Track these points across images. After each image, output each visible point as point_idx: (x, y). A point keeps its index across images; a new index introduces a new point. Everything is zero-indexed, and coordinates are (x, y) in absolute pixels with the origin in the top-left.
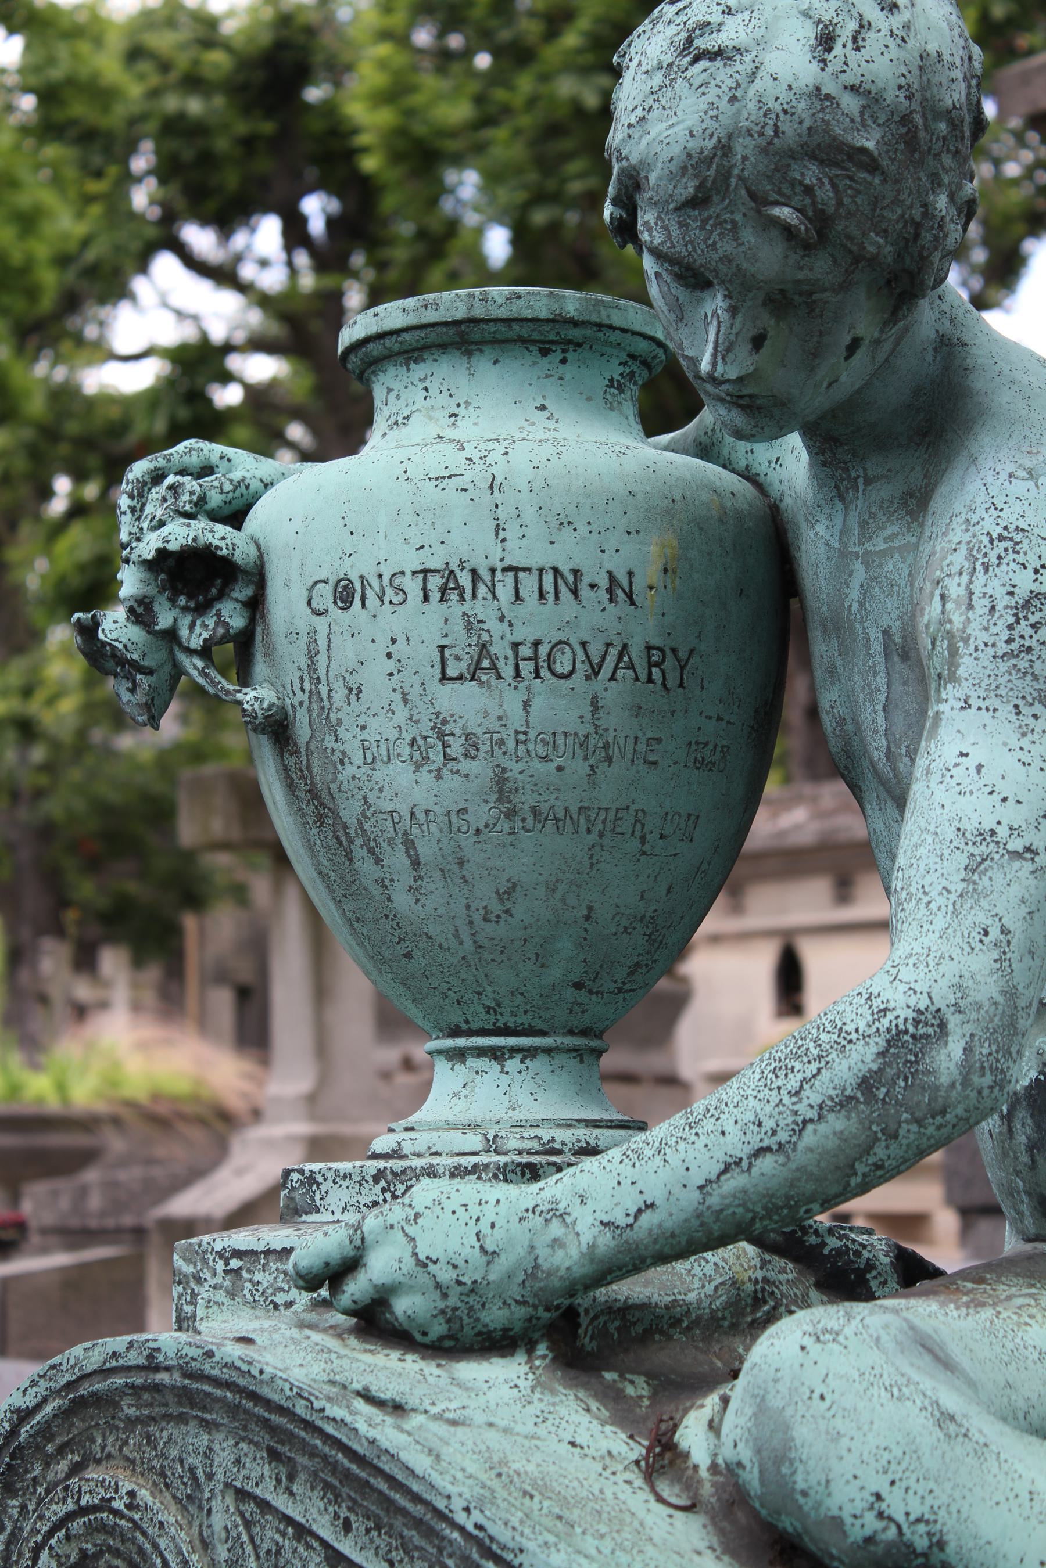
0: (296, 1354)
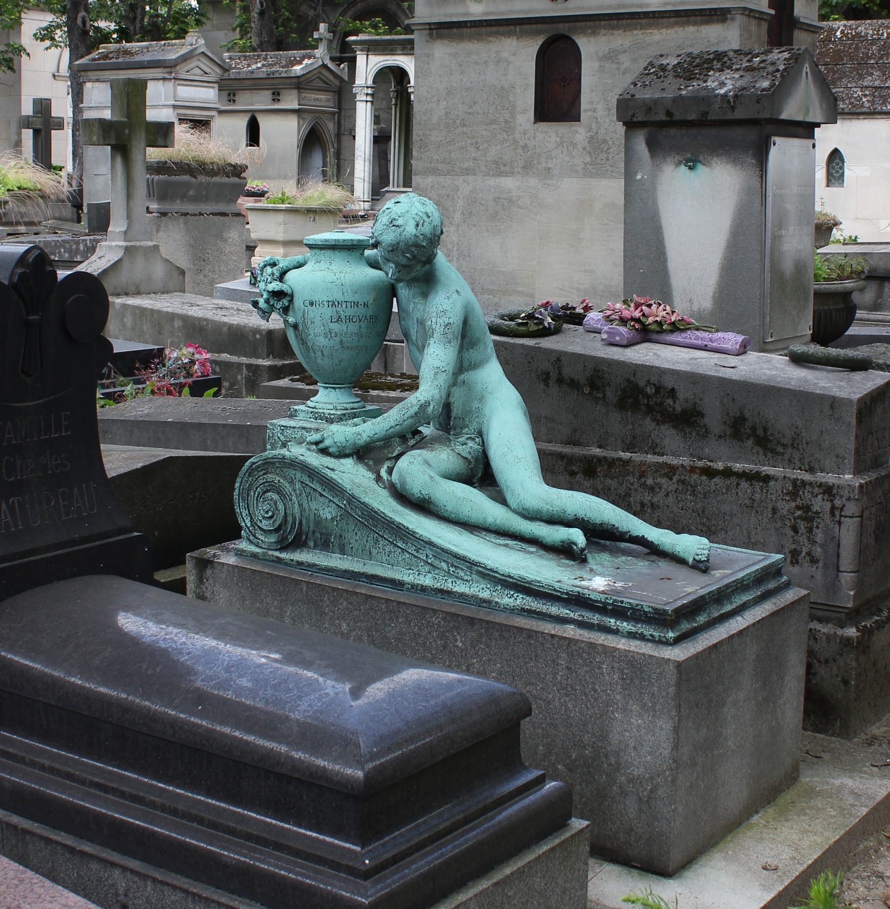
0: (314, 460)
